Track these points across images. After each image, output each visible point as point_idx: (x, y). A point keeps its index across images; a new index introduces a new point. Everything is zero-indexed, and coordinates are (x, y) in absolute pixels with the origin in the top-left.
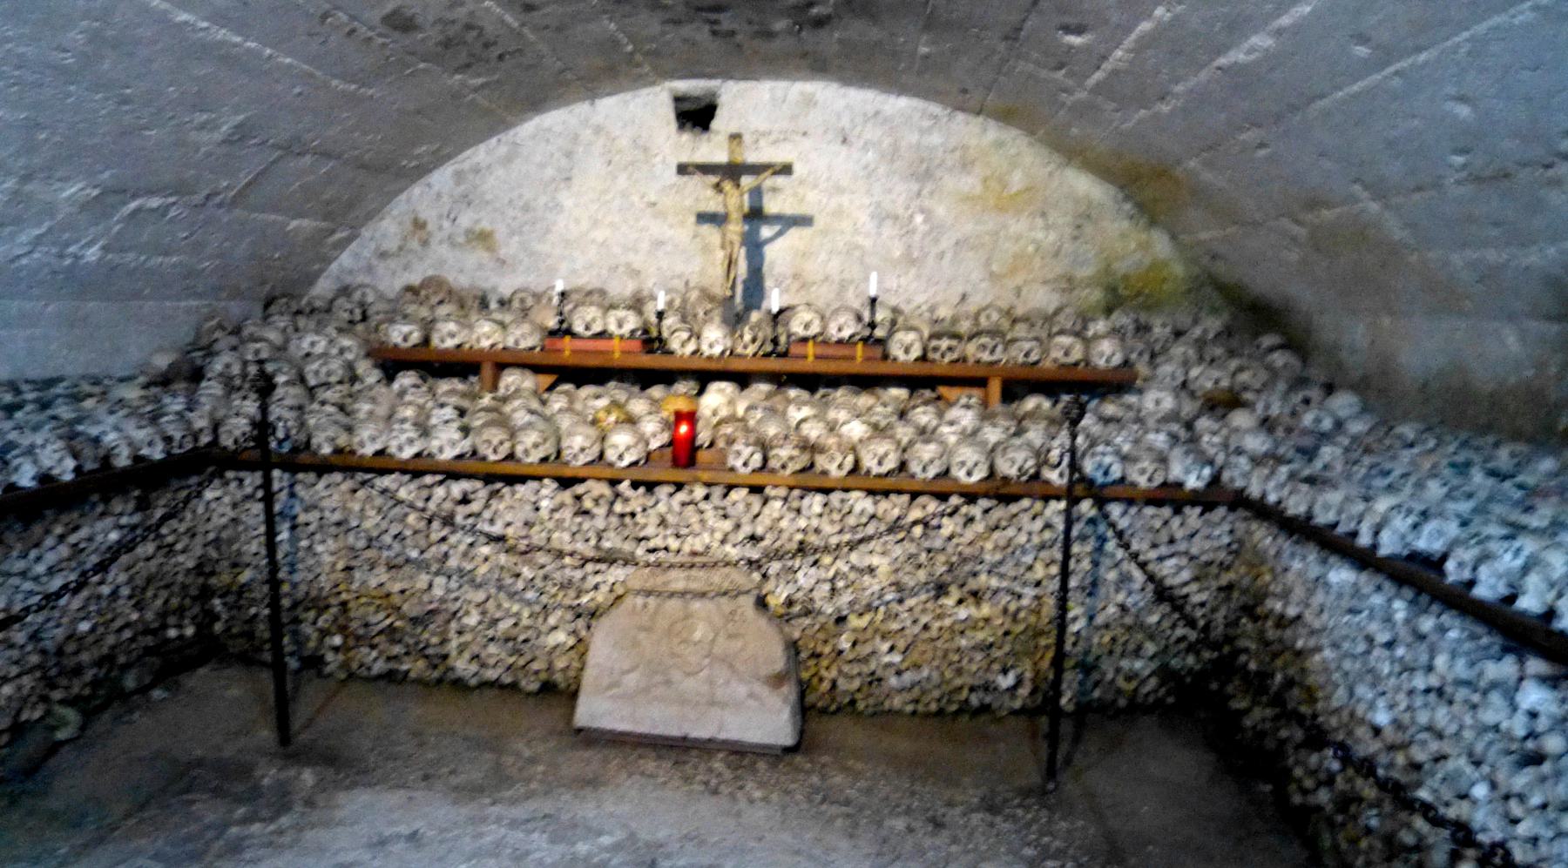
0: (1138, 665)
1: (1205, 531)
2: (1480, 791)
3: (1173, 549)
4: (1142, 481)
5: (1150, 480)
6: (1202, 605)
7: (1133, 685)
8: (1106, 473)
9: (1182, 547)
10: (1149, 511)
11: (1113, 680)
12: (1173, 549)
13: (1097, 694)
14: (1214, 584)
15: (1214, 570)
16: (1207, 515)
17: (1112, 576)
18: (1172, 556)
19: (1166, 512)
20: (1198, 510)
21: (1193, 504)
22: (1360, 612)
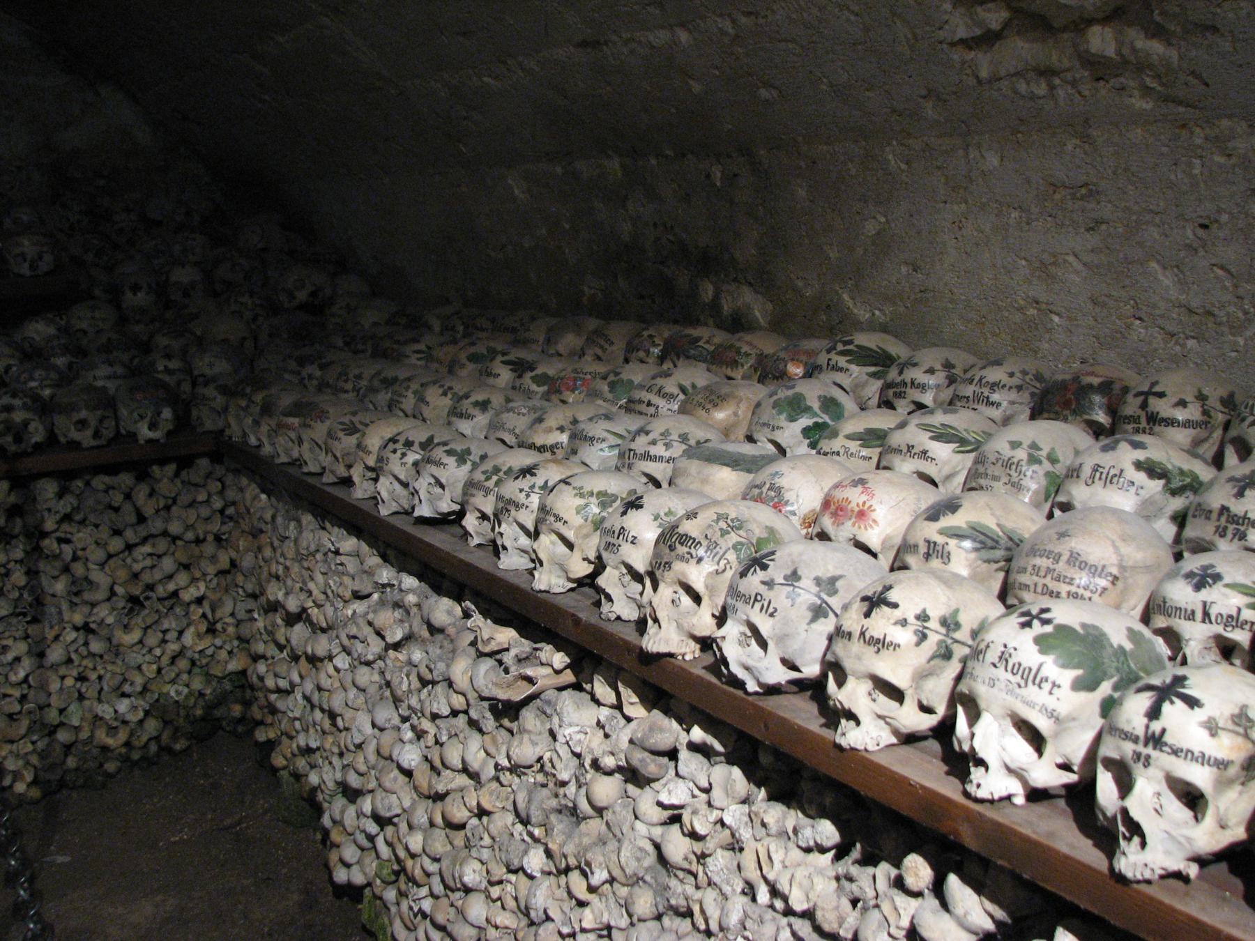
0: (123, 706)
1: (185, 499)
2: (535, 861)
3: (143, 531)
4: (85, 438)
5: (96, 435)
6: (199, 601)
7: (122, 736)
8: (18, 439)
9: (156, 525)
10: (100, 482)
11: (92, 737)
12: (143, 531)
13: (71, 762)
14: (211, 570)
15: (209, 548)
16: (184, 474)
17: (60, 587)
18: (144, 541)
19: (126, 479)
20: (171, 468)
21: (163, 462)
22: (369, 596)
